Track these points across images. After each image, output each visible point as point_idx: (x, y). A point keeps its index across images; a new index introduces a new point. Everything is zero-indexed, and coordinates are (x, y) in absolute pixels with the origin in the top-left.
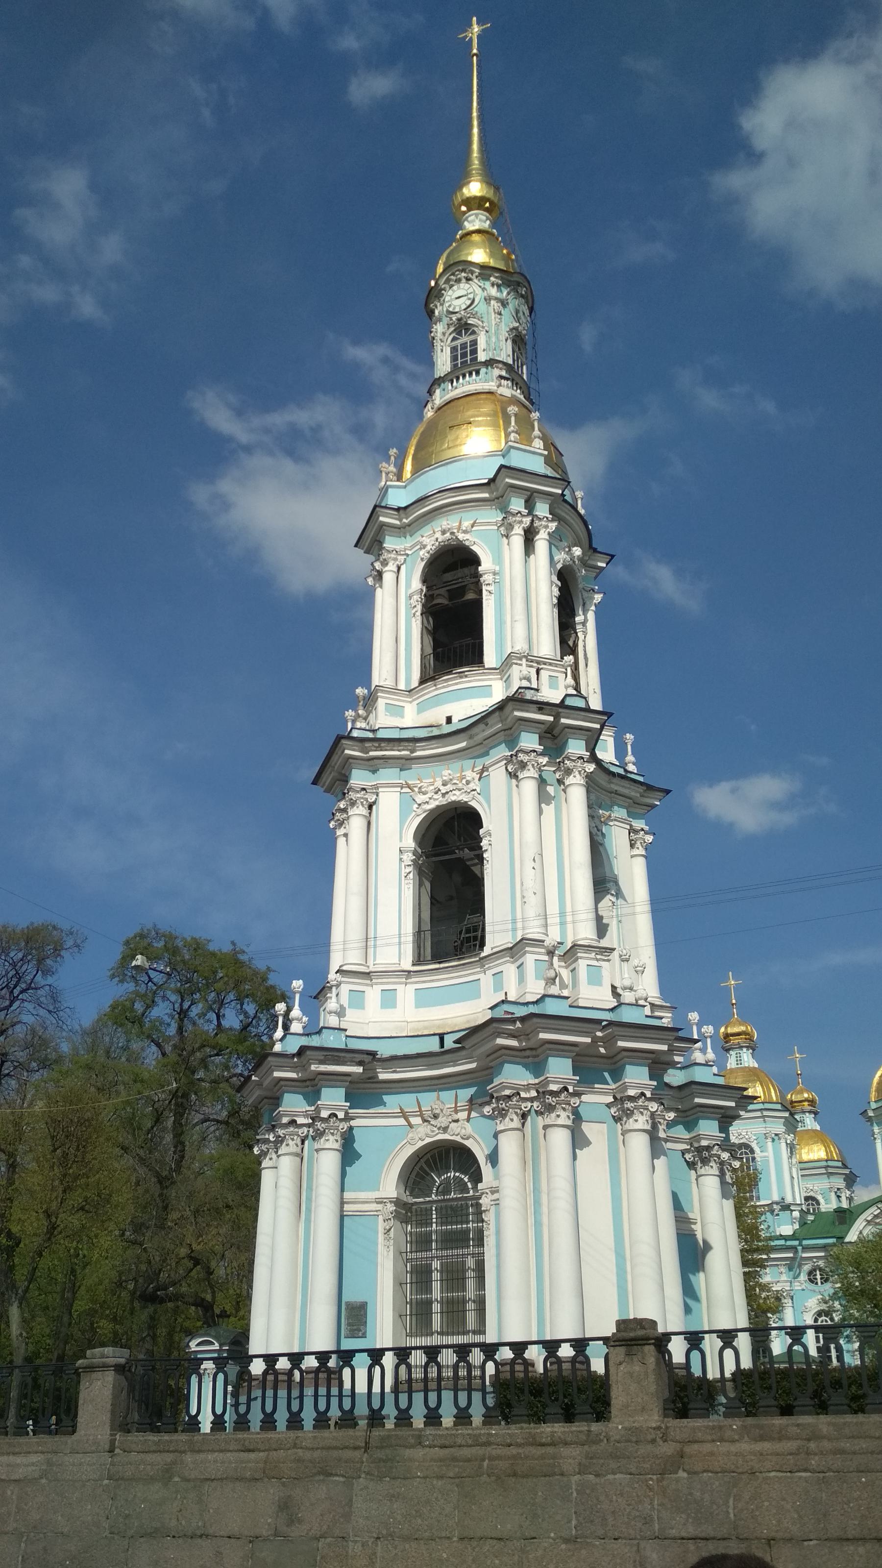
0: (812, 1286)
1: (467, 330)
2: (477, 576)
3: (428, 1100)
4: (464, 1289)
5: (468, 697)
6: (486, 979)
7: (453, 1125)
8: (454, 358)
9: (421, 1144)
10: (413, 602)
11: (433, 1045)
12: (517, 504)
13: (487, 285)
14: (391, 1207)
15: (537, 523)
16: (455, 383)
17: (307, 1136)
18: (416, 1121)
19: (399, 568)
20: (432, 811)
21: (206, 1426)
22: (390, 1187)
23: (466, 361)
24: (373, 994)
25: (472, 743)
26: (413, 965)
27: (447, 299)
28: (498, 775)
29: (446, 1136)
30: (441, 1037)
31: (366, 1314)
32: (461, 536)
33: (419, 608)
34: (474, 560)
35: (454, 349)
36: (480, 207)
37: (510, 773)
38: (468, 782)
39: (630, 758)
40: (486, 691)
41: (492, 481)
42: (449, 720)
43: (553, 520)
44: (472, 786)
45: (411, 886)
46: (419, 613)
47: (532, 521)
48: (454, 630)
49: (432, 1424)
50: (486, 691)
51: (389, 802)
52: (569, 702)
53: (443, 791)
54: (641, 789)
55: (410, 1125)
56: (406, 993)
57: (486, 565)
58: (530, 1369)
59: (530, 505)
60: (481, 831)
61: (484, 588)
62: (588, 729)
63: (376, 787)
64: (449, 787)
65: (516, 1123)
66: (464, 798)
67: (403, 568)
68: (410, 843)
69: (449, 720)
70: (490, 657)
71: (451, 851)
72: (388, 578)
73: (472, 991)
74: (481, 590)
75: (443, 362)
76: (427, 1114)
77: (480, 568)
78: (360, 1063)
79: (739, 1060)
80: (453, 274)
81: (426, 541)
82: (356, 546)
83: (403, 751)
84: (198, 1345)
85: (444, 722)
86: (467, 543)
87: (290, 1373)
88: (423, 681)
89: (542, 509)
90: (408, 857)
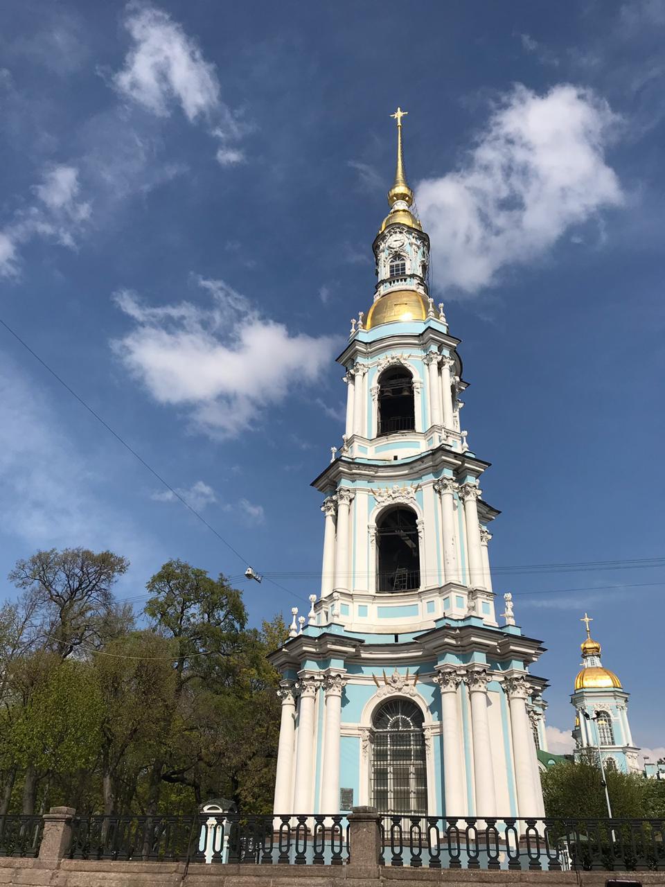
1: (399, 258)
3: (390, 672)
4: (408, 784)
5: (406, 447)
6: (422, 605)
8: (392, 271)
9: (384, 697)
10: (373, 393)
11: (391, 640)
12: (434, 348)
14: (367, 733)
15: (444, 360)
16: (392, 284)
17: (319, 687)
18: (382, 683)
19: (364, 374)
20: (386, 507)
21: (209, 859)
22: (367, 722)
23: (398, 273)
24: (354, 607)
25: (412, 471)
26: (376, 593)
28: (428, 491)
29: (400, 694)
30: (396, 636)
31: (352, 796)
32: (403, 362)
33: (377, 396)
35: (391, 267)
36: (404, 199)
37: (436, 490)
38: (408, 493)
40: (417, 444)
42: (396, 458)
43: (452, 359)
44: (411, 495)
46: (376, 399)
49: (555, 869)
50: (417, 444)
51: (362, 499)
52: (467, 454)
53: (393, 496)
54: (487, 509)
55: (378, 686)
56: (373, 608)
57: (416, 378)
58: (308, 833)
59: (440, 349)
60: (417, 521)
61: (415, 390)
62: (477, 471)
64: (397, 494)
65: (453, 689)
66: (405, 501)
67: (366, 375)
69: (396, 458)
70: (419, 426)
72: (358, 378)
73: (414, 611)
74: (413, 391)
76: (389, 680)
77: (413, 379)
78: (354, 646)
79: (593, 663)
80: (393, 229)
81: (381, 361)
82: (336, 360)
83: (370, 471)
84: (208, 809)
86: (406, 365)
87: (466, 832)
88: (378, 436)
89: (446, 352)
90: (373, 531)
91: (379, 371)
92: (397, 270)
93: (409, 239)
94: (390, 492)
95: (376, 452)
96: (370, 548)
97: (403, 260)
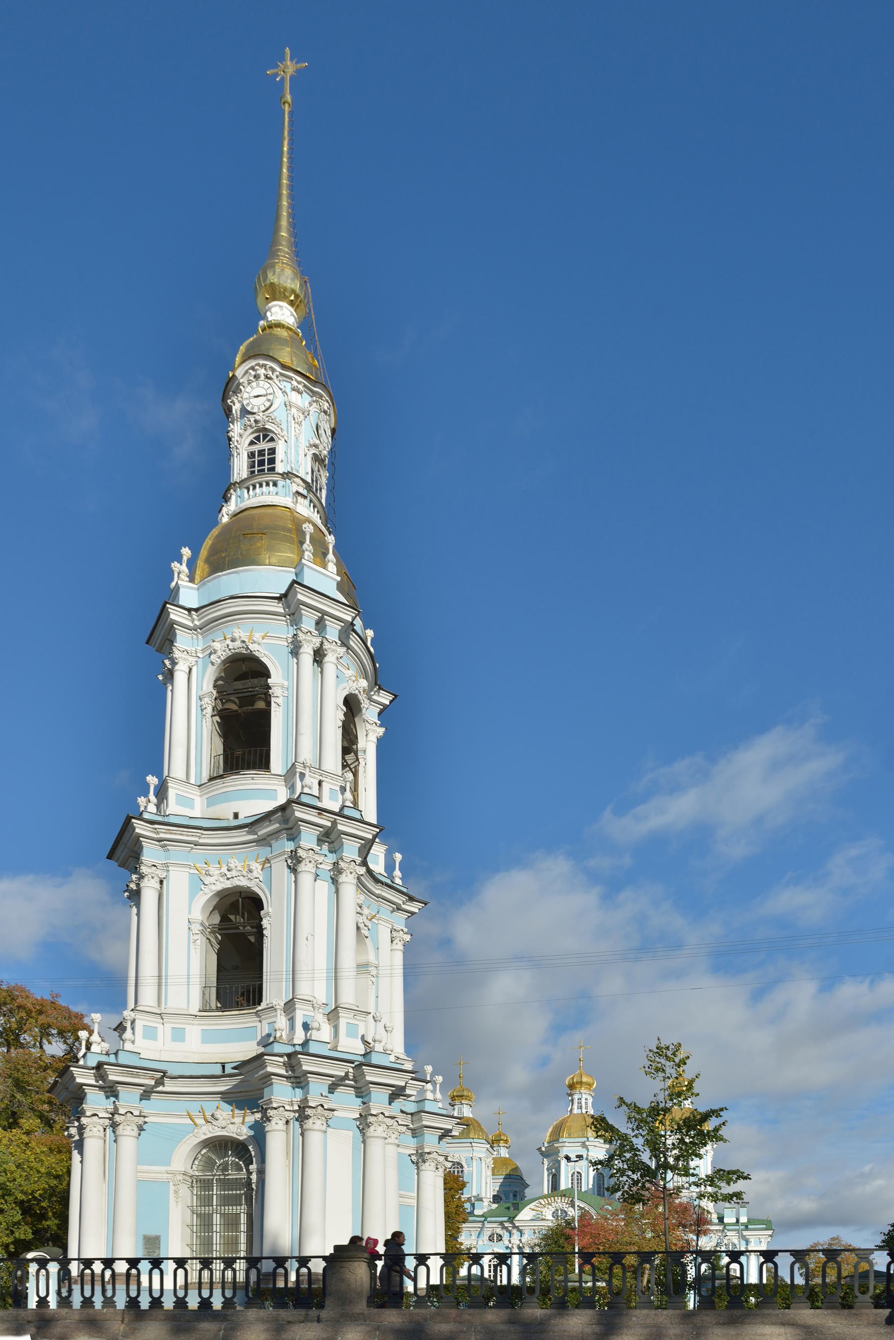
0: (491, 1243)
1: (265, 437)
7: (231, 1126)
13: (287, 386)
15: (326, 645)
16: (251, 492)
27: (245, 395)
29: (224, 1133)
31: (159, 1242)
35: (251, 455)
41: (285, 595)
42: (236, 816)
44: (255, 874)
45: (198, 951)
47: (322, 643)
48: (244, 736)
51: (179, 881)
53: (229, 876)
54: (404, 898)
55: (195, 1124)
60: (262, 913)
64: (234, 873)
69: (236, 816)
76: (209, 1118)
82: (147, 643)
85: (231, 817)
91: (213, 664)
92: (261, 463)
93: (284, 392)
95: (209, 805)
96: (193, 951)
97: (272, 440)
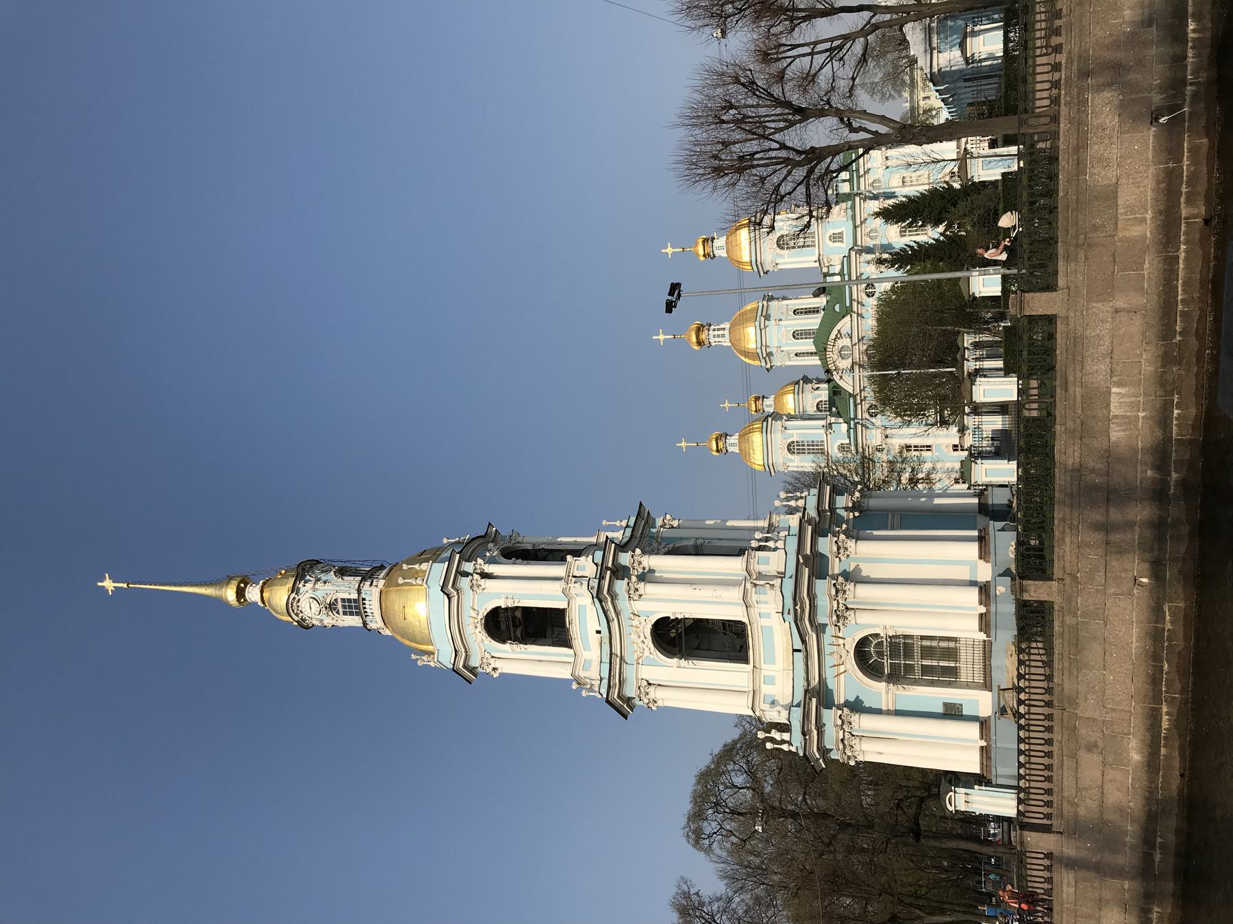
2: (507, 609)
5: (585, 618)
8: (351, 614)
23: (355, 607)
32: (481, 616)
34: (496, 612)
36: (244, 590)
39: (618, 523)
40: (582, 608)
42: (598, 632)
48: (542, 626)
50: (582, 608)
51: (647, 673)
63: (637, 680)
68: (674, 661)
69: (598, 632)
71: (678, 638)
75: (355, 621)
81: (479, 639)
83: (615, 660)
89: (468, 567)
90: (683, 662)
94: (639, 641)
